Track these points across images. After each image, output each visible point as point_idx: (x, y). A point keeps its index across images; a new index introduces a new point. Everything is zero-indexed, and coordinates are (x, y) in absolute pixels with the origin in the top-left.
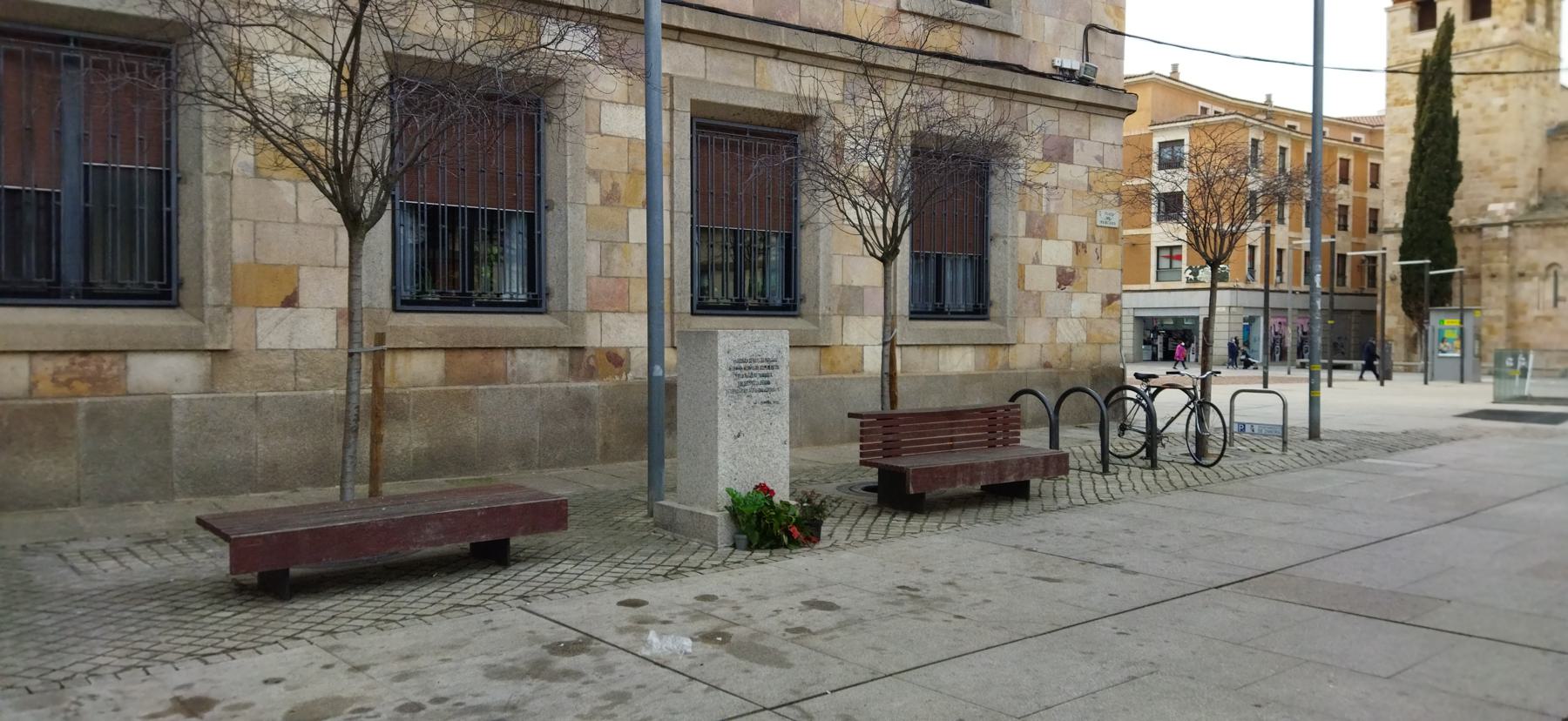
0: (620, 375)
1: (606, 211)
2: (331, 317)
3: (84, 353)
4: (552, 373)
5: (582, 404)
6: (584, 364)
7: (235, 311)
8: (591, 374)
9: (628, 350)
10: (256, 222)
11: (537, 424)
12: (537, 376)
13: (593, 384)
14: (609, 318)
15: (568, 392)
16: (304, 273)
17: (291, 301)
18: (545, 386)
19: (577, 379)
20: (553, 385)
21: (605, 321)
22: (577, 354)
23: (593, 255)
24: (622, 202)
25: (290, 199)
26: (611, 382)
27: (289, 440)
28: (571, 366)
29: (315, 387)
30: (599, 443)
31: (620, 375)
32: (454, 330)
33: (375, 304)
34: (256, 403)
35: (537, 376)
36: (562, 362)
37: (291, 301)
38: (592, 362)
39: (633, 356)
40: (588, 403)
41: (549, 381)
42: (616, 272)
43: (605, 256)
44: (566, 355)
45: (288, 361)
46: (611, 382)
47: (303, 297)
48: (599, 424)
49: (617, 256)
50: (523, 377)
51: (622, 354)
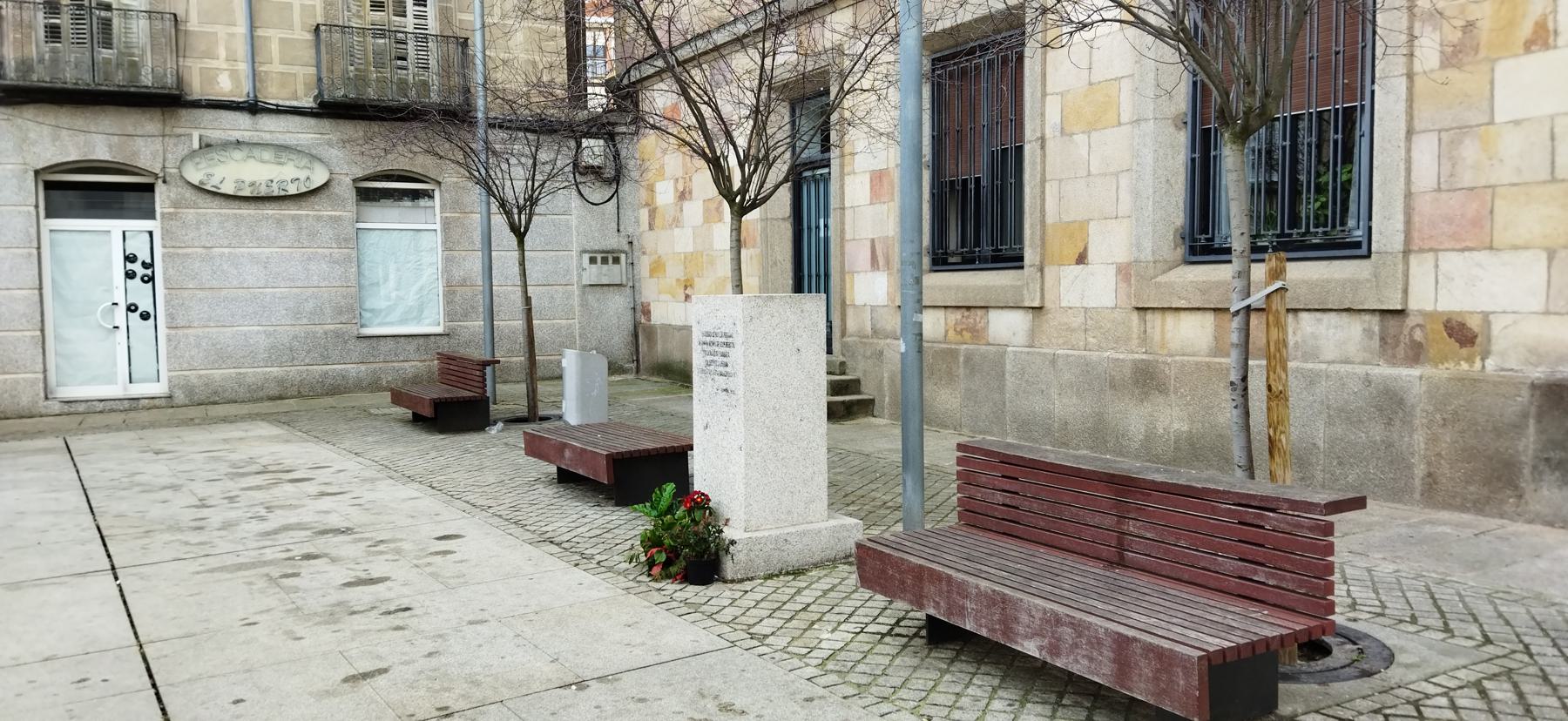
0: (1470, 360)
1: (1452, 74)
2: (1112, 270)
3: (968, 308)
4: (1352, 350)
5: (1391, 403)
6: (1405, 339)
7: (1046, 270)
8: (1416, 354)
9: (1486, 317)
10: (1060, 181)
11: (1320, 425)
12: (1330, 352)
13: (1416, 372)
14: (1451, 262)
15: (1368, 381)
16: (1093, 228)
17: (1082, 259)
18: (1337, 367)
19: (1393, 361)
20: (1349, 368)
21: (1443, 266)
22: (1392, 322)
23: (1425, 152)
24: (1482, 54)
25: (1084, 152)
26: (1441, 372)
27: (1075, 400)
28: (1382, 339)
29: (1100, 348)
30: (1420, 470)
31: (1470, 360)
32: (958, 288)
33: (1142, 257)
34: (1054, 360)
35: (1330, 352)
36: (1368, 332)
37: (1082, 259)
38: (1418, 335)
39: (1496, 329)
40: (1401, 402)
41: (1347, 361)
42: (1467, 179)
43: (1448, 154)
44: (1374, 322)
45: (1077, 321)
46: (1441, 372)
47: (1091, 256)
48: (1419, 439)
49: (1470, 151)
50: (1311, 355)
51: (1474, 323)
